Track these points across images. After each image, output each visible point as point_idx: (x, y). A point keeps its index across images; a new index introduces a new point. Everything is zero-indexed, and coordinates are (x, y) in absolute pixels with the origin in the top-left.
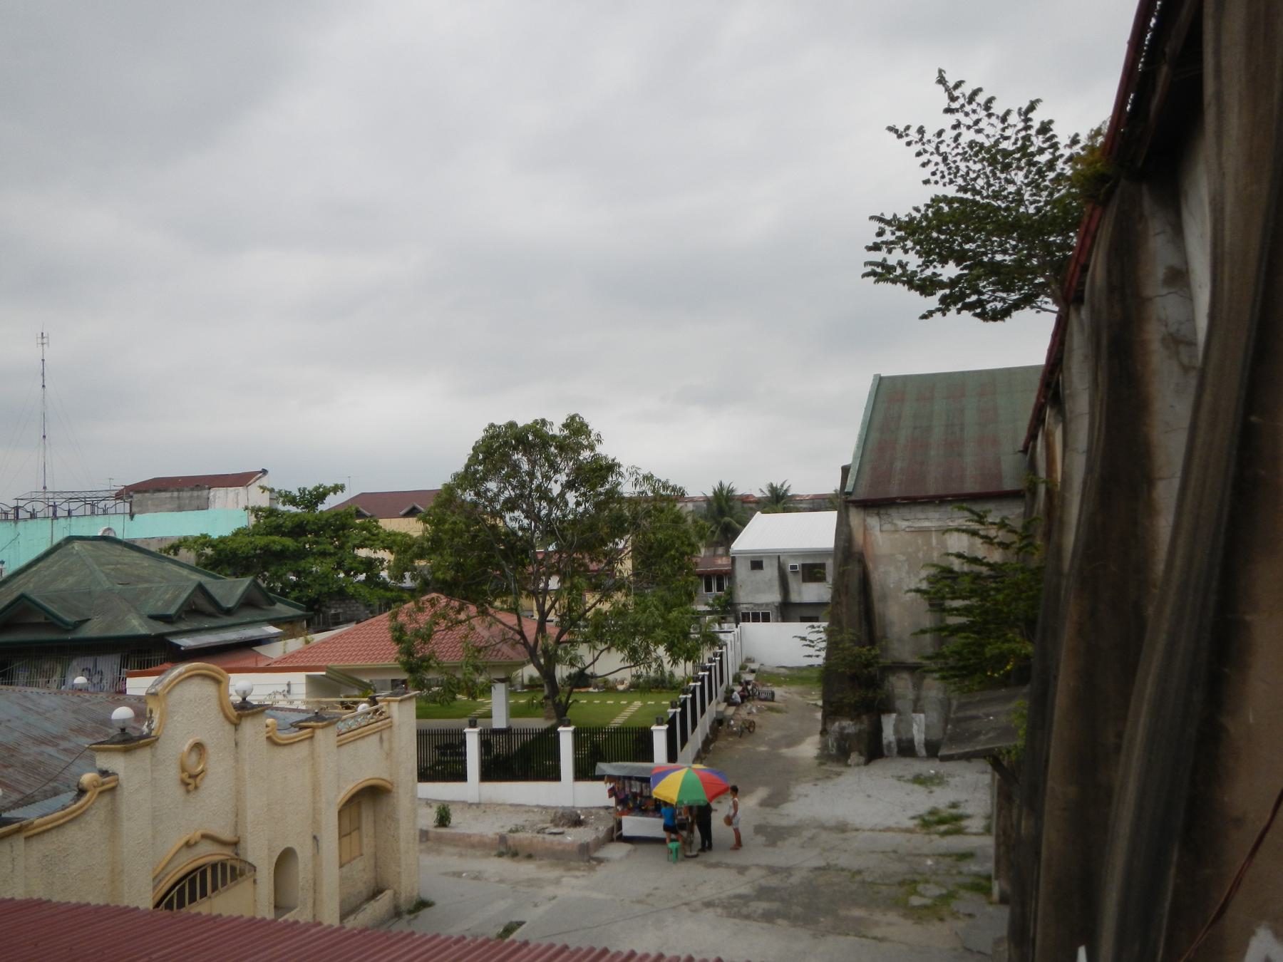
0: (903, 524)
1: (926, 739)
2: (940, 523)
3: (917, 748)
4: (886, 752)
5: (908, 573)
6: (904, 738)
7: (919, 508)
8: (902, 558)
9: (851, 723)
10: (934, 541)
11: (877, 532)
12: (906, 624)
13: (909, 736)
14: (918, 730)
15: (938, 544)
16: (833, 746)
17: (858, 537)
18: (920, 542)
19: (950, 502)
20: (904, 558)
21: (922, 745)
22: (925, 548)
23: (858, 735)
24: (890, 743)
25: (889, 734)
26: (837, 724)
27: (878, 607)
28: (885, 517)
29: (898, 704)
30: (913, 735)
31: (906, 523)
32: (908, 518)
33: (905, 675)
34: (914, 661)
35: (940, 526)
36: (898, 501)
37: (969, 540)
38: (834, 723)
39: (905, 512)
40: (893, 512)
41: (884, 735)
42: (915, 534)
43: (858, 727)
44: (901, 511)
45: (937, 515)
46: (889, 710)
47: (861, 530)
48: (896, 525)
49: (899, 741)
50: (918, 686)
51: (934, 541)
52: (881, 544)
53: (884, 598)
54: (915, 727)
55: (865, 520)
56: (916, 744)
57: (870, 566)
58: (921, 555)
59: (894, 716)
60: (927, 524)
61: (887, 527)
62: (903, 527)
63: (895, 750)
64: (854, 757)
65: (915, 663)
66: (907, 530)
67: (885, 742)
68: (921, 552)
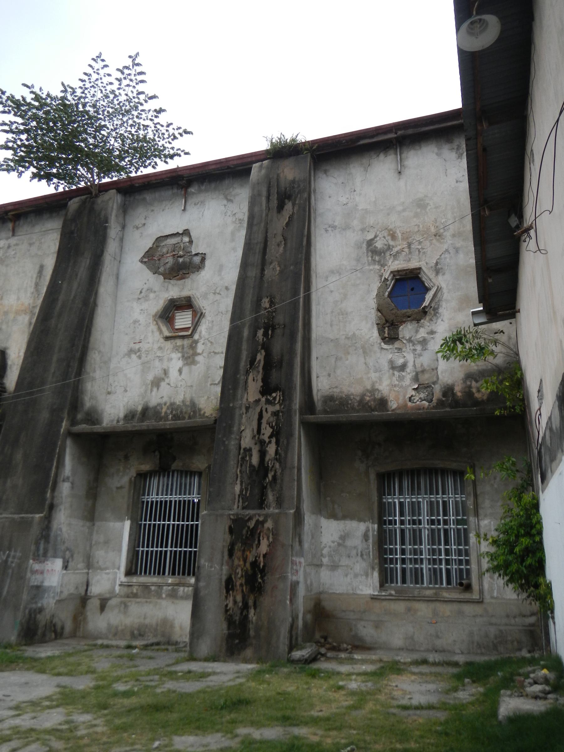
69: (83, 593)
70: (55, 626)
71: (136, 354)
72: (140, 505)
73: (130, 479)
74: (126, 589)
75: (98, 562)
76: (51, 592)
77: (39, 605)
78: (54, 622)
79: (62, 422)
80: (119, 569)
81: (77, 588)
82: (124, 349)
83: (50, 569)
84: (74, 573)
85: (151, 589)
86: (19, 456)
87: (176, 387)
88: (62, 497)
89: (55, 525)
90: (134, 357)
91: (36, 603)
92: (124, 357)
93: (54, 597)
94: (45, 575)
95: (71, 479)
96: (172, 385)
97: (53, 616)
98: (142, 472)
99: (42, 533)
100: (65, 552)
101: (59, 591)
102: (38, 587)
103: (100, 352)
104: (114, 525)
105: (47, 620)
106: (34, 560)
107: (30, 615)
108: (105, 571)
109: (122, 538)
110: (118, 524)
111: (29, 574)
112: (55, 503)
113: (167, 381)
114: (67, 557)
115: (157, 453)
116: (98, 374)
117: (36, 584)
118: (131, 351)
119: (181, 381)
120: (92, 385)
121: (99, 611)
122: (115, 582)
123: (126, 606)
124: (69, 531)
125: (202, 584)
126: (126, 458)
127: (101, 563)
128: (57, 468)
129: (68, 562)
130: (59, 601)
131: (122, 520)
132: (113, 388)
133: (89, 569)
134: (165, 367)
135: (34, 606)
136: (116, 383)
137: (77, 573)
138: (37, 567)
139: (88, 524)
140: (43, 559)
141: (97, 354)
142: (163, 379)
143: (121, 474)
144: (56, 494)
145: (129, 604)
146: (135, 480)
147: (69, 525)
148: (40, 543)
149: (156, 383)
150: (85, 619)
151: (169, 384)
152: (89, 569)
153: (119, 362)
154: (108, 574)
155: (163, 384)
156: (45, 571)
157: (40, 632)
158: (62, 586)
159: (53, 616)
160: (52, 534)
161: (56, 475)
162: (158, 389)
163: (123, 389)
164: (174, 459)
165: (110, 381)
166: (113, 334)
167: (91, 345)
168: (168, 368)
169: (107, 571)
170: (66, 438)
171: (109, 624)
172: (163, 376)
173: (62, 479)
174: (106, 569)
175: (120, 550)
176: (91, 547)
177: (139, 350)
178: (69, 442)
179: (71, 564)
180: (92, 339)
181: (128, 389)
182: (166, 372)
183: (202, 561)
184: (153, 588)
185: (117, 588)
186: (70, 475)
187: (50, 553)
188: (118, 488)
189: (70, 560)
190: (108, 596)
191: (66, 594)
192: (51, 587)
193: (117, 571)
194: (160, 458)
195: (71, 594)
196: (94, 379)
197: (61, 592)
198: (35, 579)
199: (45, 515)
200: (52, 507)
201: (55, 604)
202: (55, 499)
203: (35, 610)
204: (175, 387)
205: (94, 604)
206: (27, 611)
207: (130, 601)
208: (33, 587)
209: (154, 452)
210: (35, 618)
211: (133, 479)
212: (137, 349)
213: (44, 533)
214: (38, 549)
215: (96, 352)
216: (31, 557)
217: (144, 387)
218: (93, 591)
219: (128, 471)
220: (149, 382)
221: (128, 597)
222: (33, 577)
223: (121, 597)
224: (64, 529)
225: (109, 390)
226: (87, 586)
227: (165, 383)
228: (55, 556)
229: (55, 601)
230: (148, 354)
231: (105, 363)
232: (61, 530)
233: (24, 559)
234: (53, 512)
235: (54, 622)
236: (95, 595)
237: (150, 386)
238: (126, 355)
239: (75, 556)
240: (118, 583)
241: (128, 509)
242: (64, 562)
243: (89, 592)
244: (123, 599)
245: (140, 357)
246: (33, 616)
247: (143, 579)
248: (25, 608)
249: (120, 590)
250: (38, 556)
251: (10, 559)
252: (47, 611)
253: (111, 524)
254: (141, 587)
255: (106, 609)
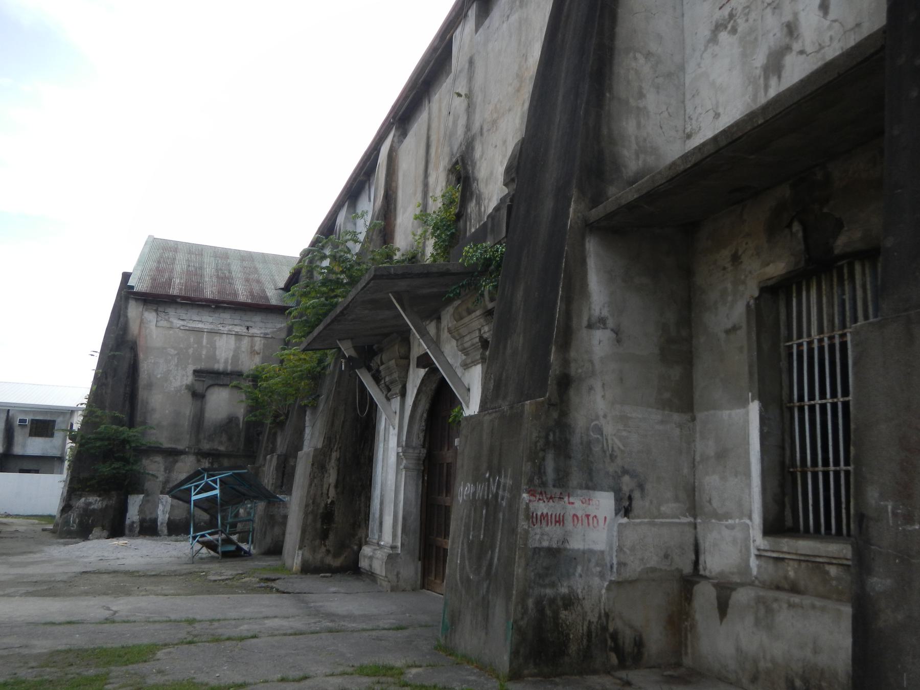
0: (179, 323)
1: (169, 519)
2: (212, 327)
3: (159, 528)
4: (127, 532)
5: (177, 365)
6: (148, 518)
7: (195, 311)
8: (173, 352)
9: (98, 499)
10: (205, 341)
11: (152, 326)
12: (167, 411)
13: (153, 516)
14: (163, 511)
15: (207, 344)
16: (74, 522)
17: (134, 327)
18: (192, 340)
19: (225, 309)
20: (176, 352)
21: (165, 525)
22: (196, 346)
23: (104, 511)
24: (133, 523)
25: (133, 514)
26: (83, 500)
27: (142, 394)
28: (163, 315)
29: (148, 485)
30: (157, 515)
31: (182, 323)
32: (184, 317)
33: (159, 459)
34: (169, 446)
35: (211, 329)
36: (179, 300)
37: (235, 344)
38: (79, 499)
39: (182, 312)
40: (171, 312)
41: (128, 515)
42: (188, 332)
43: (105, 503)
44: (179, 311)
45: (210, 319)
46: (138, 492)
47: (138, 321)
48: (172, 322)
49: (142, 521)
50: (169, 469)
51: (205, 341)
52: (155, 337)
53: (150, 386)
54: (161, 507)
55: (142, 315)
56: (159, 524)
57: (141, 356)
58: (191, 351)
59: (141, 496)
60: (200, 325)
61: (163, 323)
62: (178, 325)
63: (138, 529)
64: (96, 531)
65: (169, 448)
66: (182, 328)
67: (128, 522)
68: (192, 349)
69: (688, 569)
70: (614, 636)
71: (726, 27)
72: (784, 364)
73: (748, 306)
74: (770, 567)
75: (710, 501)
76: (592, 564)
77: (564, 590)
78: (611, 629)
79: (569, 206)
80: (750, 518)
81: (666, 556)
82: (705, 32)
83: (580, 514)
84: (653, 524)
85: (827, 573)
86: (520, 294)
87: (821, 47)
88: (591, 362)
89: (580, 420)
90: (723, 36)
91: (553, 585)
92: (705, 50)
93: (602, 576)
94: (569, 525)
95: (610, 323)
96: (809, 49)
97: (607, 615)
98: (770, 283)
99: (547, 437)
100: (617, 477)
101: (615, 562)
102: (553, 552)
103: (648, 55)
104: (729, 415)
105: (590, 623)
106: (532, 493)
107: (541, 610)
108: (724, 522)
109: (748, 443)
110: (737, 413)
111: (523, 524)
112: (573, 372)
113: (796, 47)
114: (626, 489)
115: (796, 227)
116: (651, 101)
117: (545, 544)
118: (718, 27)
119: (830, 28)
120: (639, 125)
121: (716, 614)
122: (748, 549)
123: (769, 611)
124: (624, 434)
125: (879, 583)
126: (736, 259)
127: (716, 504)
128: (568, 300)
129: (630, 498)
130: (619, 583)
131: (744, 404)
132: (694, 122)
133: (695, 519)
134: (787, 17)
135: (549, 592)
136: (699, 110)
137: (662, 524)
138: (541, 507)
139: (676, 417)
140: (557, 491)
141: (641, 60)
142: (788, 48)
143: (730, 298)
144: (573, 354)
145: (775, 606)
146: (757, 306)
147: (623, 419)
148: (544, 459)
149: (774, 65)
150: (693, 627)
151: (802, 52)
152: (695, 517)
153: (699, 65)
154: (731, 527)
155: (790, 60)
156: (569, 519)
157: (573, 648)
158: (620, 549)
159: (607, 615)
160: (576, 440)
161: (568, 315)
162: (779, 77)
163: (711, 114)
164: (839, 226)
165: (688, 111)
166: (683, 15)
167: (620, 43)
168: (796, 15)
169: (730, 521)
170: (583, 238)
171: (739, 649)
172: (787, 40)
173: (585, 322)
174: (727, 516)
175: (748, 475)
176: (693, 466)
177: (731, 16)
178: (592, 246)
179: (637, 504)
180: (622, 30)
181: (721, 110)
182: (791, 29)
183: (872, 495)
184: (833, 571)
185: (753, 563)
186: (605, 313)
187: (576, 477)
188: (727, 332)
189: (637, 495)
190: (736, 579)
191: (635, 567)
192: (591, 551)
193: (748, 521)
194: (806, 238)
195: (653, 570)
196: (641, 111)
197: (621, 564)
198: (542, 534)
199: (549, 399)
200: (565, 382)
201: (608, 589)
202: (573, 365)
203: (552, 601)
204: (817, 52)
205: (705, 594)
206: (530, 603)
207: (776, 600)
208: (537, 551)
209: (789, 226)
210: (556, 616)
211: (752, 302)
212: (727, 17)
213: (551, 437)
214: (540, 471)
215: (638, 55)
216: (524, 487)
217: (750, 88)
218: (709, 565)
219: (741, 288)
220: (758, 72)
221: (778, 588)
222: (537, 529)
223: (765, 586)
224: (609, 429)
225: (688, 130)
226: (697, 552)
227: (794, 53)
228: (591, 485)
229: (606, 584)
230: (748, 13)
231: (669, 75)
232: (599, 430)
233: (515, 491)
234: (572, 392)
235: (611, 629)
236: (713, 574)
237: (762, 81)
238: (709, 41)
239: (648, 486)
240: (753, 551)
241: (751, 374)
242: (618, 500)
243: (701, 567)
244: (762, 593)
245: (734, 31)
246: (548, 612)
247: (805, 546)
248: (524, 596)
249: (759, 567)
250: (544, 484)
251: (501, 492)
252: (587, 605)
253: (725, 414)
254: (803, 565)
255: (729, 611)
